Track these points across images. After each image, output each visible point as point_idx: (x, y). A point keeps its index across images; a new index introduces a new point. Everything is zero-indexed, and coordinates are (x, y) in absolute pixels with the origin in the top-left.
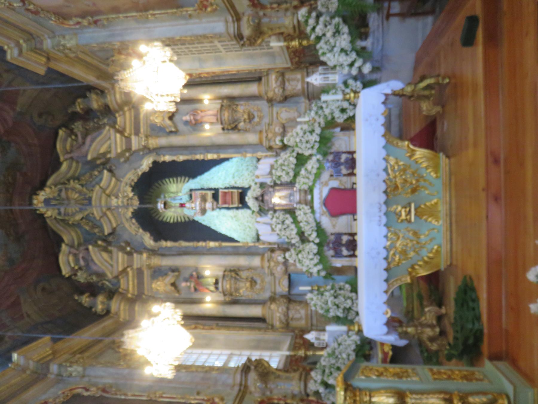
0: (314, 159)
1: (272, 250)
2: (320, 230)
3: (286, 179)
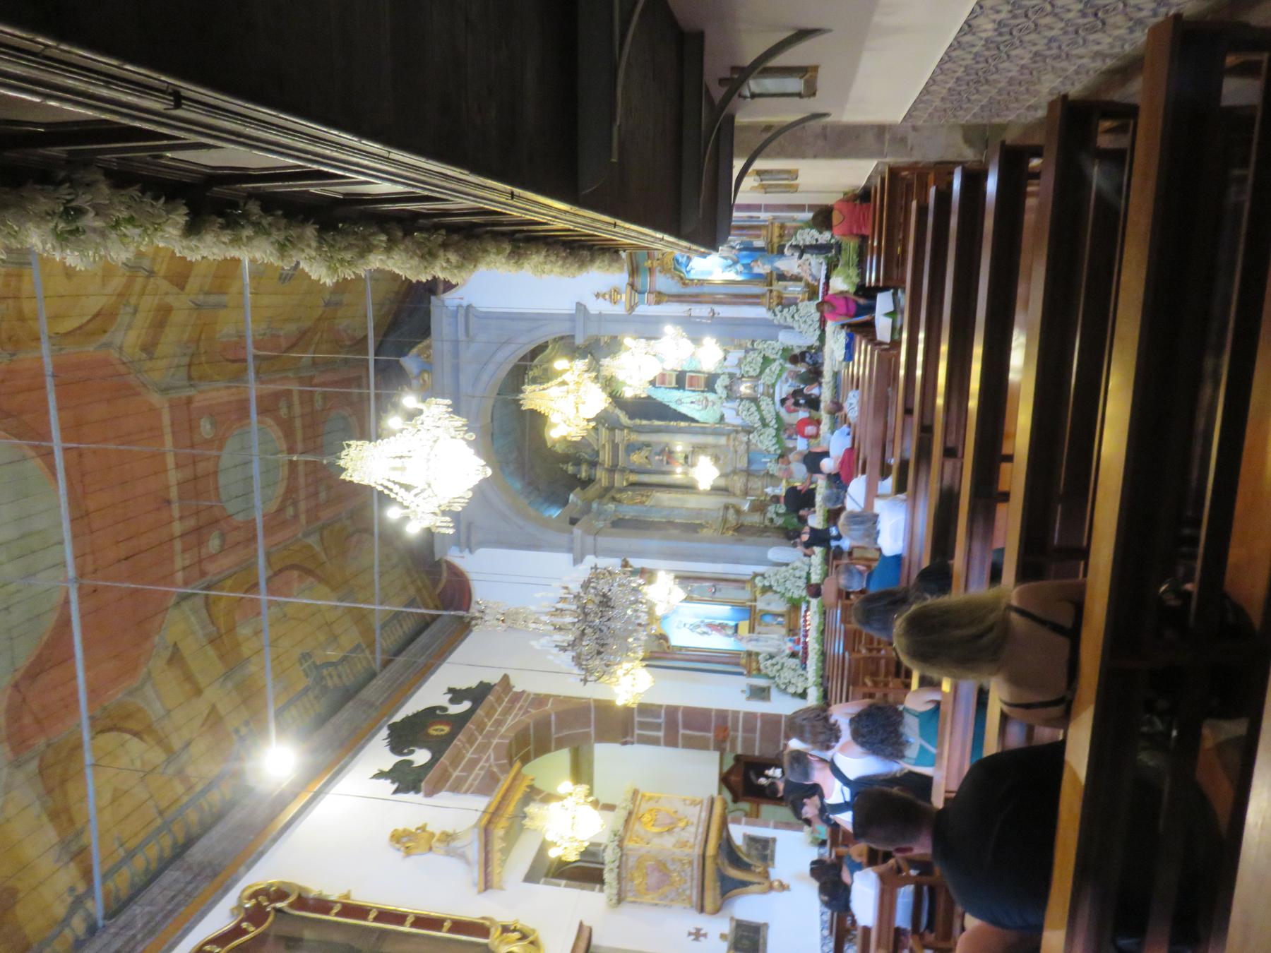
0: (777, 363)
1: (737, 432)
2: (778, 418)
3: (752, 373)
